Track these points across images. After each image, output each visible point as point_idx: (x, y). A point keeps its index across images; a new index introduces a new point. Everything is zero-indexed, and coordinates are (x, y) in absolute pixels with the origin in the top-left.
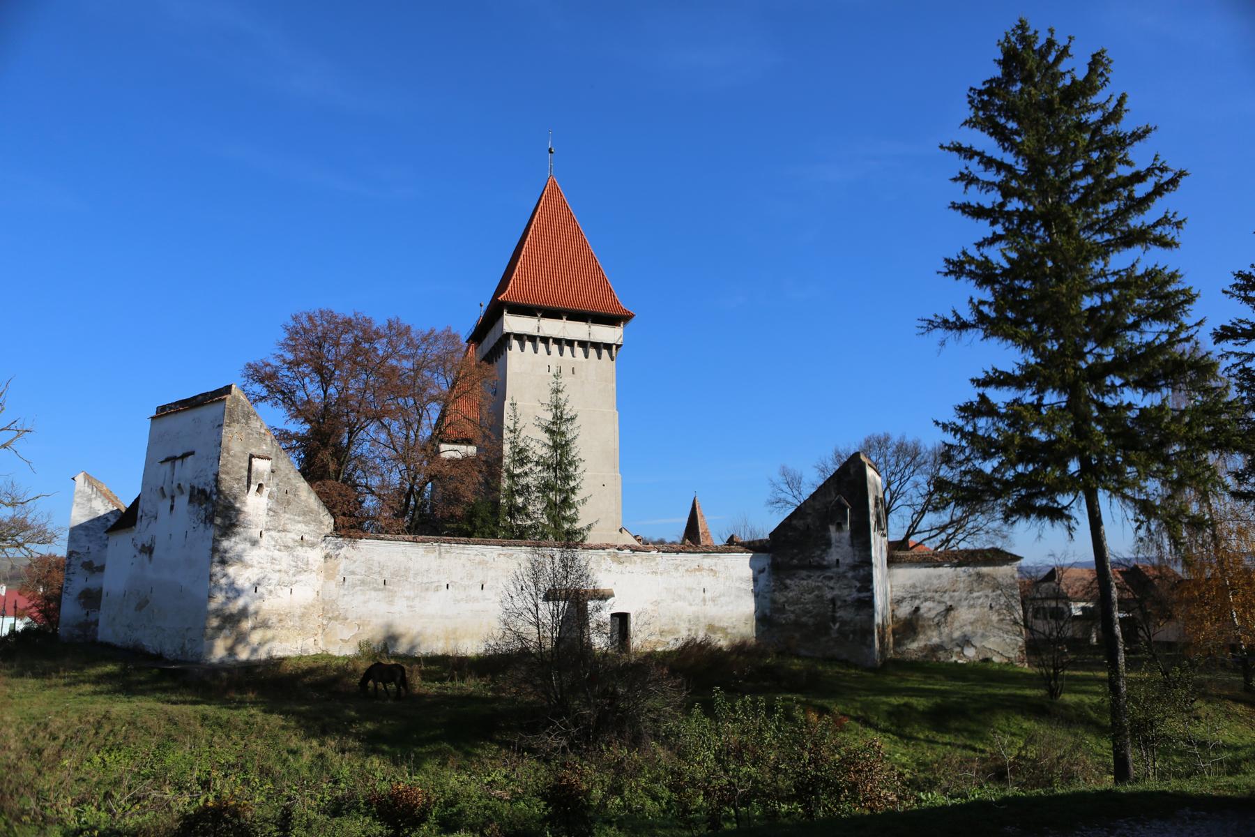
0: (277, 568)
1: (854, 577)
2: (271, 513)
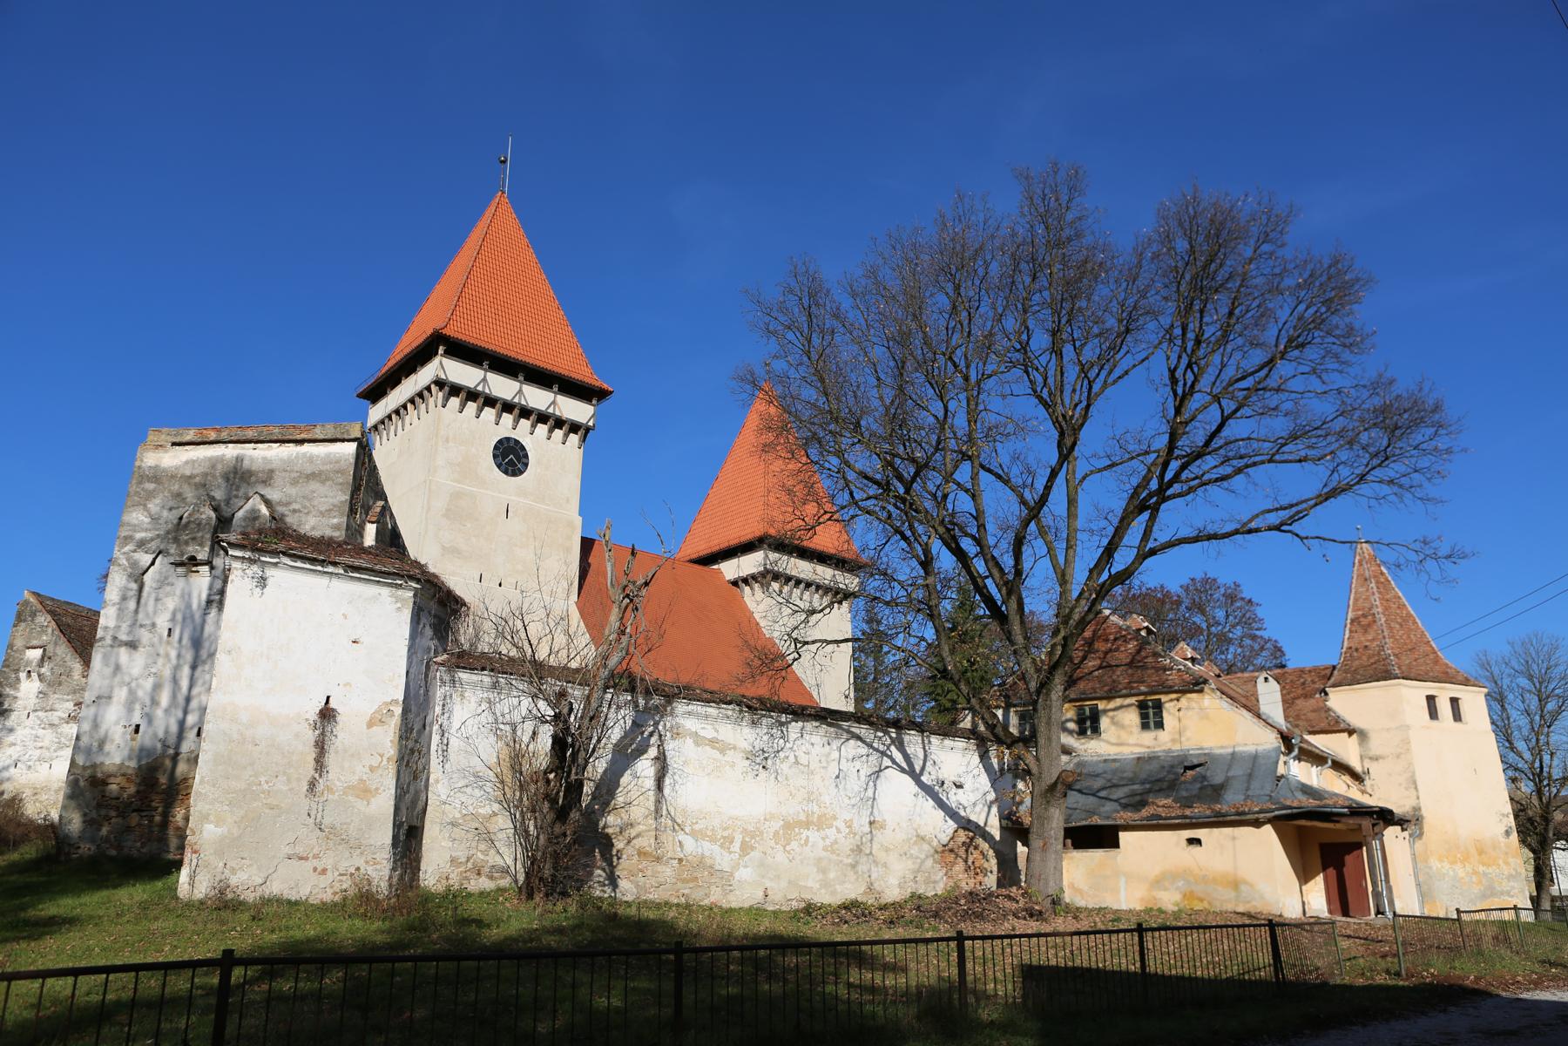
0: (40, 744)
2: (41, 696)
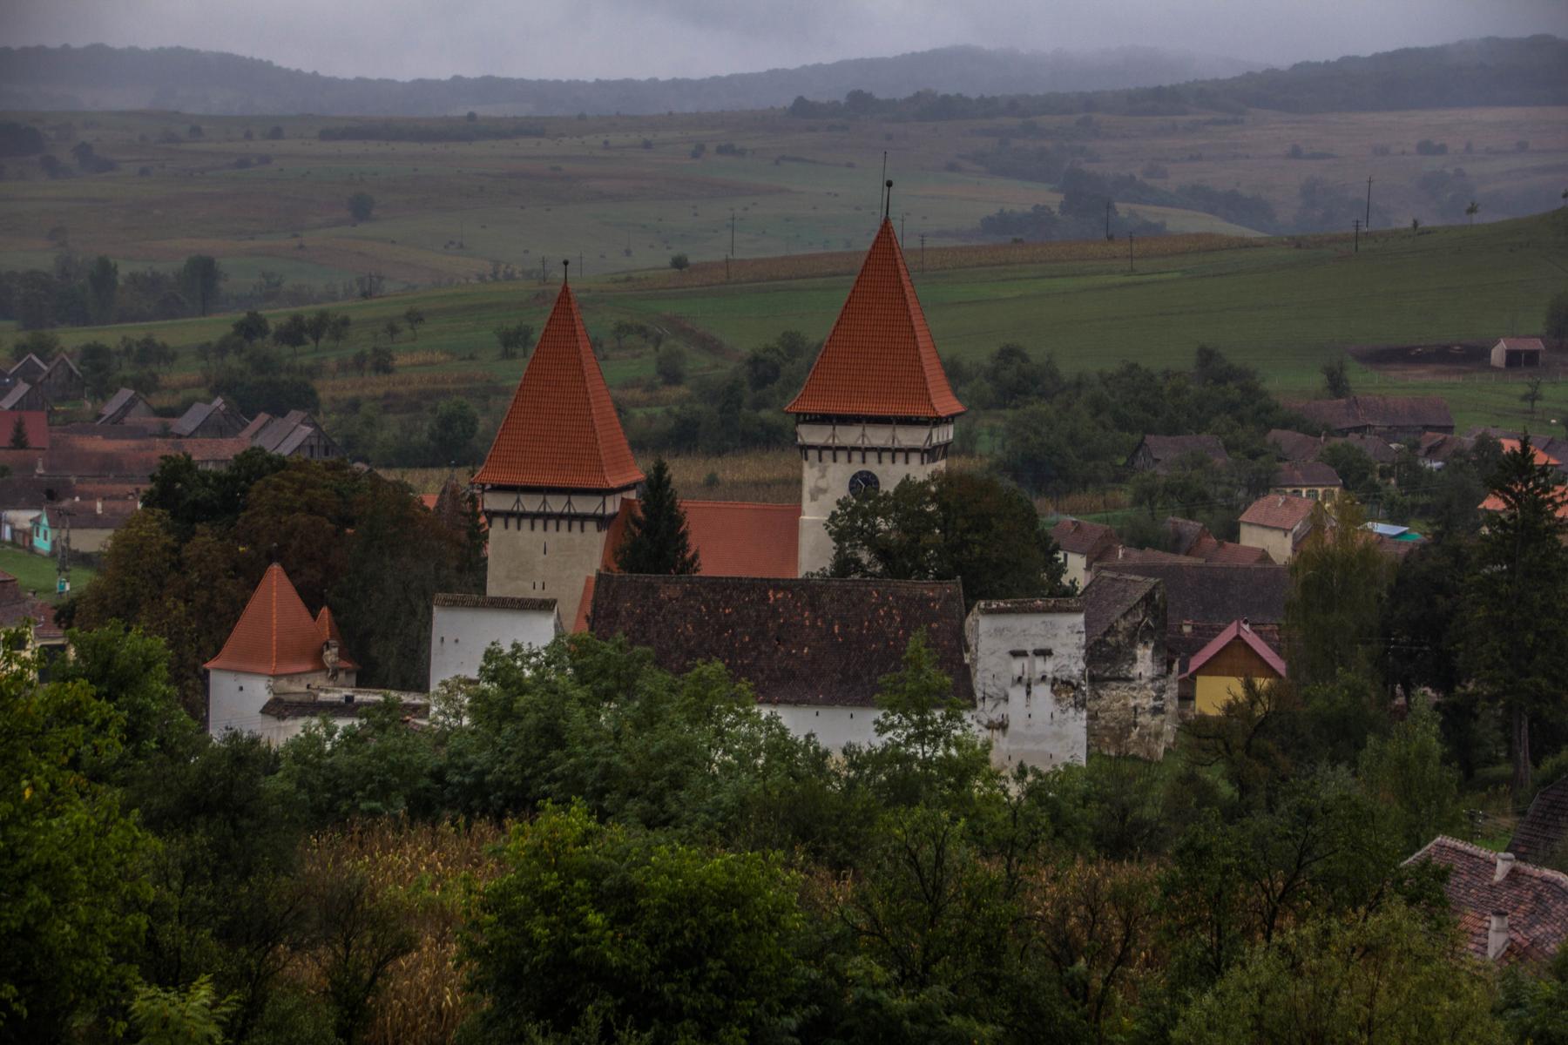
1: (1152, 689)
